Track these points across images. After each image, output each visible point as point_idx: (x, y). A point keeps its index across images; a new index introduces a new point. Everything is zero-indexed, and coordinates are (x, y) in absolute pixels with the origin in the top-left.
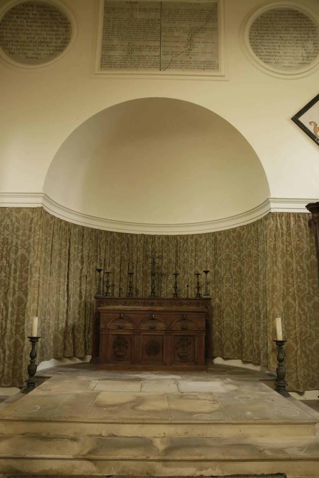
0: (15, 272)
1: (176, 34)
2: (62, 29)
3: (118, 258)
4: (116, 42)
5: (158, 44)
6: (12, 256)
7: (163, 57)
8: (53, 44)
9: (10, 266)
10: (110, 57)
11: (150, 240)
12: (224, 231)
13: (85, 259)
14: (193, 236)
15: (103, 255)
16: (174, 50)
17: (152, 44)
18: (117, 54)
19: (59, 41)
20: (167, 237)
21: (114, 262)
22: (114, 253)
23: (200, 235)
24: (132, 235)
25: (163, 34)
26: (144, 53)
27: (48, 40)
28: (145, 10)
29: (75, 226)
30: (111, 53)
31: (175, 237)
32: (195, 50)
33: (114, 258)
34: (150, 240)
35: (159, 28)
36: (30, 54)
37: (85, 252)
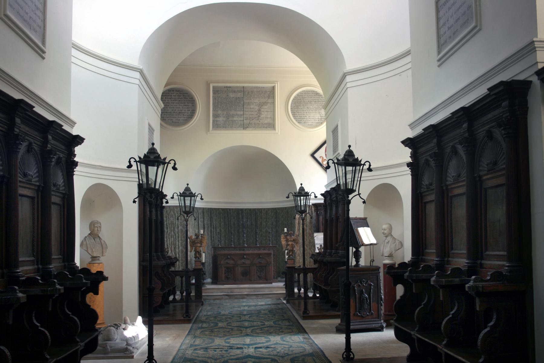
0: (178, 237)
1: (252, 107)
2: (190, 105)
3: (222, 224)
4: (220, 112)
5: (242, 113)
6: (176, 230)
7: (245, 121)
8: (186, 114)
9: (176, 235)
10: (217, 121)
11: (240, 212)
12: (281, 208)
13: (206, 226)
14: (264, 209)
15: (214, 223)
16: (251, 116)
17: (239, 113)
18: (221, 119)
19: (189, 112)
20: (250, 210)
21: (220, 226)
22: (220, 221)
23: (269, 209)
24: (230, 209)
25: (245, 106)
26: (235, 119)
27: (183, 111)
28: (234, 92)
29: (200, 208)
30: (218, 119)
31: (254, 210)
32: (262, 116)
33: (220, 224)
34: (240, 212)
35: (242, 103)
36: (174, 120)
37: (205, 222)
